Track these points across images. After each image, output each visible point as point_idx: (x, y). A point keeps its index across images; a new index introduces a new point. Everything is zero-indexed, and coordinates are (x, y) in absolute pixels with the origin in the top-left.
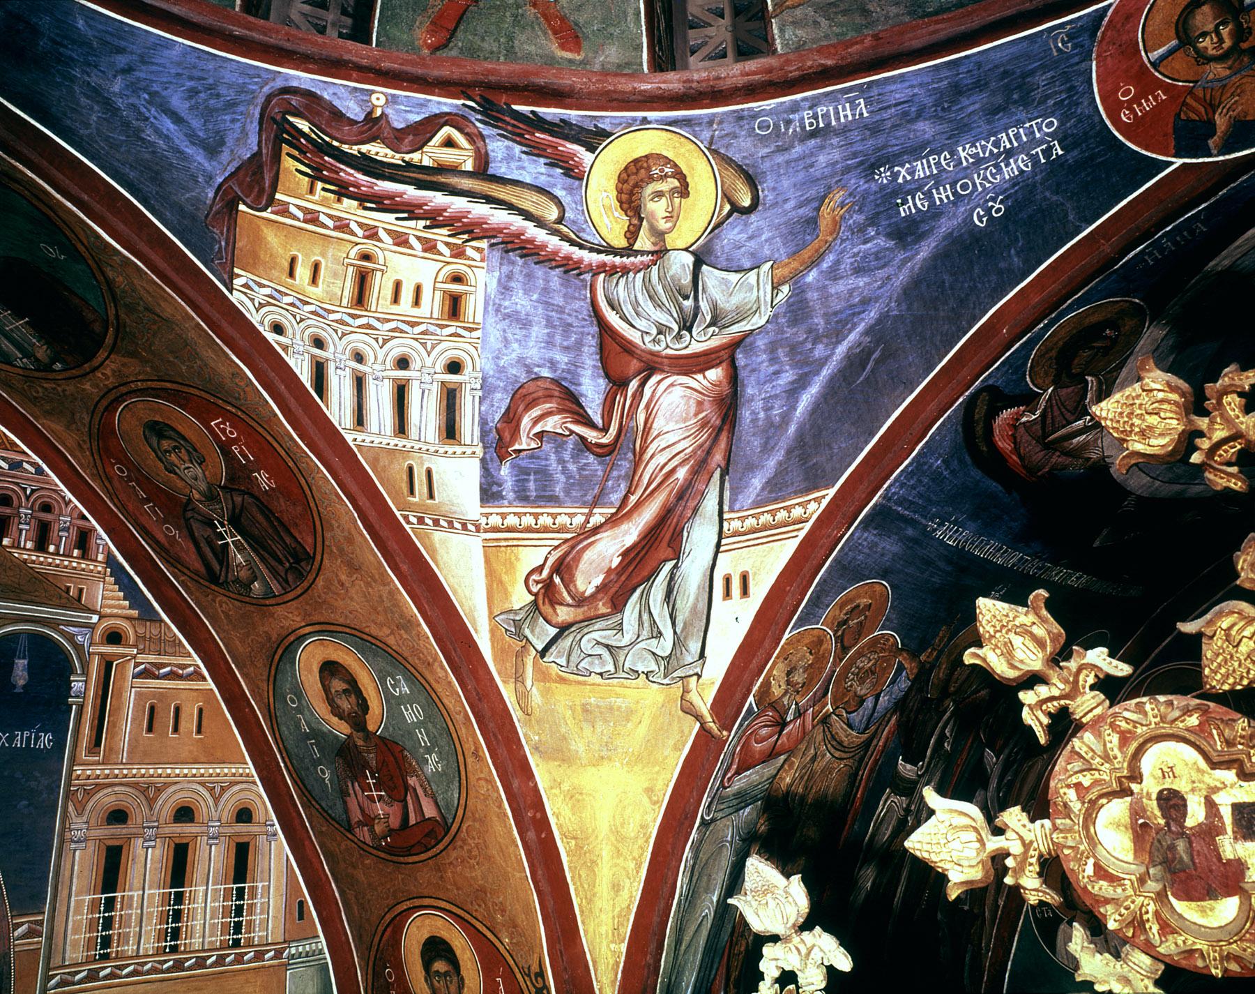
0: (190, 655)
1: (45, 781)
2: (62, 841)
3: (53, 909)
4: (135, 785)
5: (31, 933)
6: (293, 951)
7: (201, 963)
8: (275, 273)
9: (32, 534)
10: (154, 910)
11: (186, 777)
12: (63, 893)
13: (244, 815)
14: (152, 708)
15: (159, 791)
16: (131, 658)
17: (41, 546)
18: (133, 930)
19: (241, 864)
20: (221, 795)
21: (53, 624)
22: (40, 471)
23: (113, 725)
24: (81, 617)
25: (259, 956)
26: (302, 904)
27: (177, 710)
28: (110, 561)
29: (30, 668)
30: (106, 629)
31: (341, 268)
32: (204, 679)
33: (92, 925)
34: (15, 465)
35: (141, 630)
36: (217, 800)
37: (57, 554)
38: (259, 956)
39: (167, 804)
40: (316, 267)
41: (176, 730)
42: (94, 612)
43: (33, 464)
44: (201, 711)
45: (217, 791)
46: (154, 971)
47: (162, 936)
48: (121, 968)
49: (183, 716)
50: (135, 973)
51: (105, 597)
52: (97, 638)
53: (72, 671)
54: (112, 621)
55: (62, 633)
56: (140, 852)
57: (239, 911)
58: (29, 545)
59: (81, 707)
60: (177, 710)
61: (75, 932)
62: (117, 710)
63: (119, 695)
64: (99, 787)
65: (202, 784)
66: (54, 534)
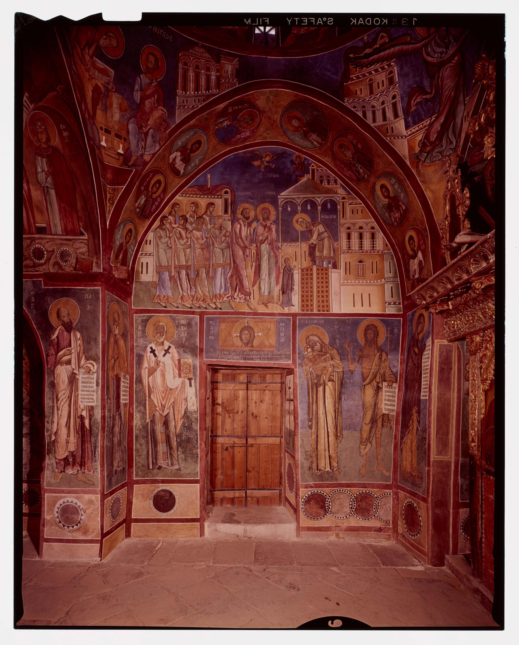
7: (367, 252)
11: (361, 222)
16: (347, 202)
17: (329, 184)
19: (373, 236)
21: (333, 197)
24: (337, 195)
25: (378, 252)
26: (387, 244)
28: (341, 184)
33: (347, 245)
36: (367, 225)
38: (378, 252)
39: (357, 226)
45: (367, 224)
51: (341, 192)
57: (373, 244)
62: (346, 211)
63: (346, 208)
64: (345, 224)
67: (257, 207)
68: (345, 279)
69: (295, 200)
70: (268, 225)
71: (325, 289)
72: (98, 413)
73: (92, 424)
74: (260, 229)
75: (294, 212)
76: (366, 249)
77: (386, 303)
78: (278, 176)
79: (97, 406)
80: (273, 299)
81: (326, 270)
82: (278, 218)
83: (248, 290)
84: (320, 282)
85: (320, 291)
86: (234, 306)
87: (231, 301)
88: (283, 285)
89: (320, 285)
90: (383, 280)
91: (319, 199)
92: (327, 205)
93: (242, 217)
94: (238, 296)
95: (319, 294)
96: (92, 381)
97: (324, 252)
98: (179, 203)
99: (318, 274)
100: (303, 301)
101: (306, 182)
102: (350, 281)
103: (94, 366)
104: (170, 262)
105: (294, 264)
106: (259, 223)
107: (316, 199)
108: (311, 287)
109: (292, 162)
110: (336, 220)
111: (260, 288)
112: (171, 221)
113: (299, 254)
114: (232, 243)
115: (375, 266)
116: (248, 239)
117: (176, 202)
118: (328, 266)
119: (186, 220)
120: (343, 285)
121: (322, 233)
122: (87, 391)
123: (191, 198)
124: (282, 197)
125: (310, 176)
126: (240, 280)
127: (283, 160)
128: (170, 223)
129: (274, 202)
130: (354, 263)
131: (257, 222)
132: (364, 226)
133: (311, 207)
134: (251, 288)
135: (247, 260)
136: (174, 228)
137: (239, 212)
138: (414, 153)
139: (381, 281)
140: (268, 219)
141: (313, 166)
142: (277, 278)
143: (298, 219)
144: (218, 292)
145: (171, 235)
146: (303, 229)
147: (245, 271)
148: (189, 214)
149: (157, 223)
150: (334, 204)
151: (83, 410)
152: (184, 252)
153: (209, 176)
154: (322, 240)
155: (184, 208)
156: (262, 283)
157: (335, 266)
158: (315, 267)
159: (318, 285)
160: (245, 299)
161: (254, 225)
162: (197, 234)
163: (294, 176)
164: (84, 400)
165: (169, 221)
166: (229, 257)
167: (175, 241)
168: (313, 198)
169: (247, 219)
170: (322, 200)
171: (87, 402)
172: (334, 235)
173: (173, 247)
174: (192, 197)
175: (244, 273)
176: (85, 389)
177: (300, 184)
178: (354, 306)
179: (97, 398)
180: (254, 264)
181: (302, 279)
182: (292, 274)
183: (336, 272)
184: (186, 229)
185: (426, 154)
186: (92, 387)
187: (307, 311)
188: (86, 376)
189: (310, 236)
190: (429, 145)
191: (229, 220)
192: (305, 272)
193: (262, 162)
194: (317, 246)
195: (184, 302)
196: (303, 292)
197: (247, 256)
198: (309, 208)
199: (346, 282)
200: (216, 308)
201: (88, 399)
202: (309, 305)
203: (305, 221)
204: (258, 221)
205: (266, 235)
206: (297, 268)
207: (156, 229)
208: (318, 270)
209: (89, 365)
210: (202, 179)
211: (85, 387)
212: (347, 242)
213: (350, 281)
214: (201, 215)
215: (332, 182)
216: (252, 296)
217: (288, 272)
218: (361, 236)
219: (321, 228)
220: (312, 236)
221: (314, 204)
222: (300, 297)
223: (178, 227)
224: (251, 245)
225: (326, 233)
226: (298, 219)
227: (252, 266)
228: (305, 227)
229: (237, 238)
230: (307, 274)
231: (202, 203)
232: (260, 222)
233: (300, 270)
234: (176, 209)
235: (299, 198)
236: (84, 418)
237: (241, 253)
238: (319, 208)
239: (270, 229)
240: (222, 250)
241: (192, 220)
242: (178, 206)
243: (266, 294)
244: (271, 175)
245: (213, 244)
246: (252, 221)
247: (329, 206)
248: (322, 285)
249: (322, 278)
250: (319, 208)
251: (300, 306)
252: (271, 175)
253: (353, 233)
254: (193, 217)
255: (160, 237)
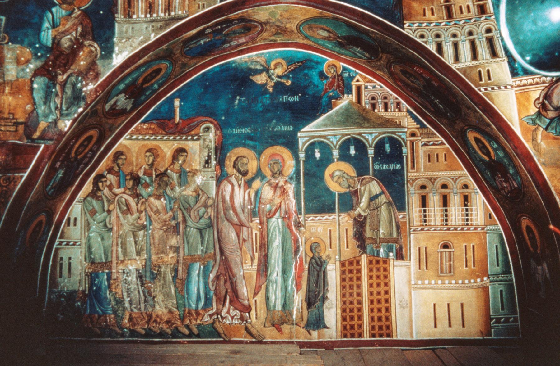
0: (438, 137)
1: (400, 178)
2: (408, 194)
3: (409, 211)
4: (427, 178)
5: (403, 217)
6: (488, 228)
7: (456, 229)
8: (419, 17)
9: (383, 107)
10: (439, 213)
11: (444, 175)
12: (411, 208)
13: (466, 186)
14: (429, 155)
15: (435, 180)
17: (386, 109)
18: (433, 218)
20: (456, 181)
21: (394, 133)
22: (381, 87)
23: (418, 161)
25: (476, 229)
26: (490, 215)
27: (437, 155)
28: (408, 111)
29: (390, 147)
30: (410, 132)
31: (440, 8)
32: (445, 144)
33: (420, 216)
34: (374, 87)
35: (421, 131)
36: (455, 182)
37: (391, 111)
38: (476, 229)
39: (438, 183)
40: (432, 9)
41: (438, 161)
42: (405, 127)
43: (379, 85)
44: (445, 155)
45: (455, 180)
46: (440, 230)
47: (442, 220)
48: (431, 228)
49: (440, 157)
50: (435, 230)
51: (408, 123)
52: (408, 136)
53: (402, 146)
54: (412, 130)
55: (398, 136)
56: (432, 198)
58: (383, 110)
59: (407, 156)
60: (437, 155)
61: (416, 217)
62: (418, 156)
63: (417, 152)
64: (416, 179)
65: (449, 177)
66: (389, 106)
67: (260, 154)
68: (419, 278)
69: (328, 139)
70: (280, 184)
71: (383, 297)
74: (267, 193)
75: (327, 160)
76: (454, 223)
77: (492, 319)
78: (296, 99)
80: (291, 315)
81: (385, 262)
82: (298, 172)
83: (246, 302)
84: (375, 285)
85: (375, 301)
86: (221, 331)
87: (217, 323)
88: (309, 291)
89: (375, 290)
90: (485, 278)
91: (371, 136)
92: (384, 147)
93: (235, 171)
94: (228, 312)
95: (373, 306)
97: (381, 231)
98: (124, 150)
99: (371, 270)
100: (344, 319)
101: (347, 109)
102: (427, 282)
104: (109, 255)
105: (327, 253)
106: (264, 182)
107: (364, 137)
108: (359, 294)
109: (322, 75)
110: (399, 173)
111: (267, 298)
112: (111, 184)
113: (335, 235)
114: (217, 218)
115: (470, 253)
116: (246, 211)
117: (119, 150)
118: (388, 256)
119: (137, 180)
120: (415, 289)
121: (377, 196)
123: (146, 142)
124: (304, 134)
125: (353, 97)
126: (232, 283)
127: (306, 71)
128: (110, 187)
129: (291, 143)
130: (435, 249)
131: (261, 180)
132: (450, 183)
133: (356, 150)
134: (251, 299)
135: (244, 248)
136: (116, 195)
137: (229, 163)
138: (529, 114)
139: (482, 280)
140: (281, 173)
141: (358, 81)
142: (298, 277)
143: (333, 173)
144: (194, 306)
145: (111, 207)
146: (343, 190)
147: (240, 267)
148: (142, 170)
149: (88, 187)
150: (396, 145)
152: (135, 236)
153: (177, 103)
154: (378, 207)
155: (134, 159)
156: (270, 288)
157: (400, 256)
158: (364, 260)
159: (372, 289)
160: (242, 318)
161: (256, 184)
162: (158, 204)
163: (325, 99)
165: (108, 183)
166: (211, 243)
167: (118, 217)
168: (360, 134)
169: (245, 174)
170: (376, 137)
172: (399, 201)
173: (115, 228)
174: (148, 139)
175: (239, 272)
177: (337, 112)
178: (435, 326)
180: (257, 255)
181: (343, 280)
182: (325, 272)
183: (401, 266)
184: (137, 196)
185: (548, 121)
187: (353, 336)
189: (354, 202)
190: (552, 109)
191: (212, 177)
192: (348, 267)
193: (270, 77)
194: (368, 220)
195: (134, 325)
196: (345, 303)
197: (244, 240)
198: (352, 152)
199: (420, 282)
200: (190, 336)
202: (356, 326)
203: (345, 175)
204: (263, 177)
205: (277, 201)
206: (332, 260)
207: (85, 199)
208: (370, 262)
210: (165, 109)
212: (420, 211)
213: (427, 282)
214: (162, 170)
215: (392, 106)
216: (253, 312)
217: (318, 268)
218: (445, 201)
219: (375, 187)
220: (358, 203)
221: (361, 146)
222: (339, 311)
223: (124, 193)
224: (252, 221)
225: (383, 196)
226: (333, 173)
227: (252, 260)
228: (347, 185)
229: (226, 209)
230: (351, 271)
231: (166, 150)
232: (267, 180)
233: (338, 263)
234: (120, 162)
235: (335, 135)
237: (233, 235)
238: (371, 152)
239: (284, 192)
240: (200, 231)
241: (148, 179)
242: (123, 157)
243: (279, 307)
244: (285, 98)
245: (185, 221)
246: (253, 179)
247: (388, 148)
248: (378, 289)
249: (378, 277)
250: (371, 152)
251: (339, 329)
252: (285, 98)
253: (431, 195)
254: (150, 175)
255: (93, 213)
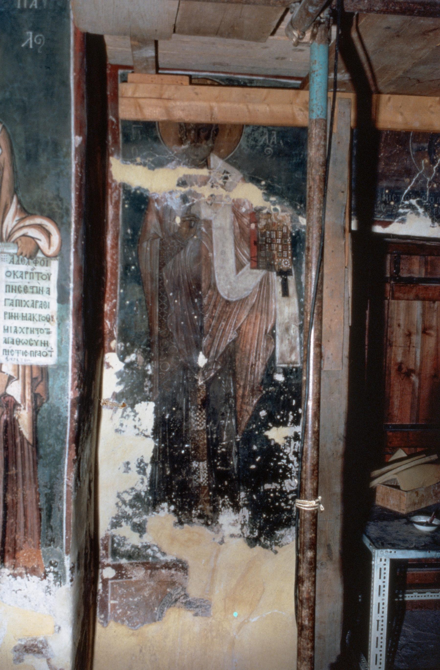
72: (63, 389)
73: (40, 424)
79: (61, 366)
96: (43, 284)
103: (48, 235)
122: (24, 317)
151: (10, 379)
164: (15, 347)
171: (25, 353)
176: (17, 310)
179: (60, 342)
186: (45, 305)
188: (23, 268)
201: (30, 343)
209: (33, 233)
211: (20, 303)
236: (16, 404)
